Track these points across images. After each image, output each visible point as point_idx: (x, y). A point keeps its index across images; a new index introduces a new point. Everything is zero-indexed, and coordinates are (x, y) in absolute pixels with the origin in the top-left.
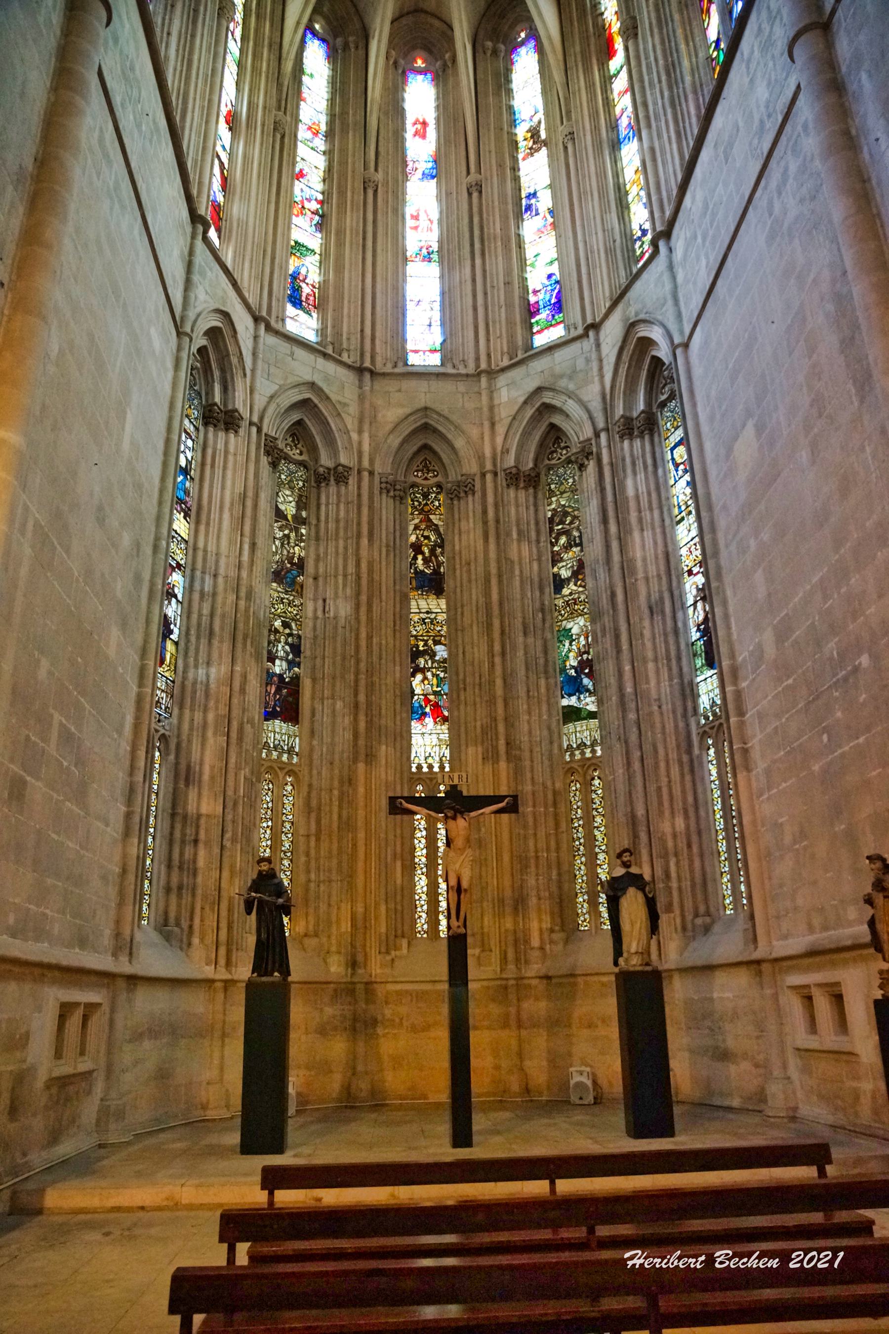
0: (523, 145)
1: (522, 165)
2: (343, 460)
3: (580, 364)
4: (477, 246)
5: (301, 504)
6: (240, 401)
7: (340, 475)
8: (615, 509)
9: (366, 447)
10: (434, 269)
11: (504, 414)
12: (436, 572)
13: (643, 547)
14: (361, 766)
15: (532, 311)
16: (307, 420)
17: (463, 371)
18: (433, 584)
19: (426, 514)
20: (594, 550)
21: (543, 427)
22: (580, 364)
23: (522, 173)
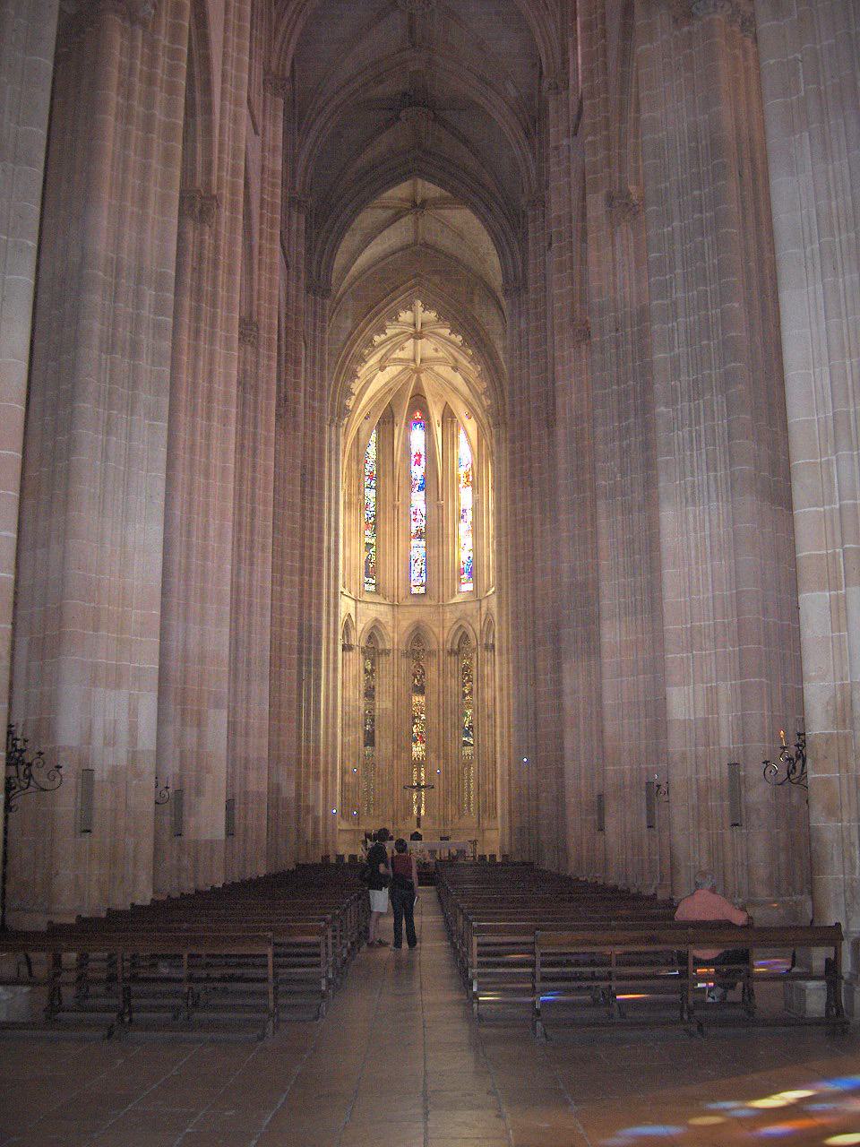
0: (462, 479)
1: (462, 490)
2: (388, 647)
3: (475, 613)
4: (441, 540)
5: (372, 665)
6: (354, 642)
7: (386, 652)
8: (481, 677)
9: (396, 640)
10: (423, 543)
11: (448, 624)
12: (422, 685)
13: (488, 694)
14: (395, 761)
15: (462, 572)
16: (374, 634)
17: (433, 603)
18: (420, 690)
19: (418, 659)
20: (475, 687)
21: (460, 633)
22: (475, 613)
23: (462, 495)
